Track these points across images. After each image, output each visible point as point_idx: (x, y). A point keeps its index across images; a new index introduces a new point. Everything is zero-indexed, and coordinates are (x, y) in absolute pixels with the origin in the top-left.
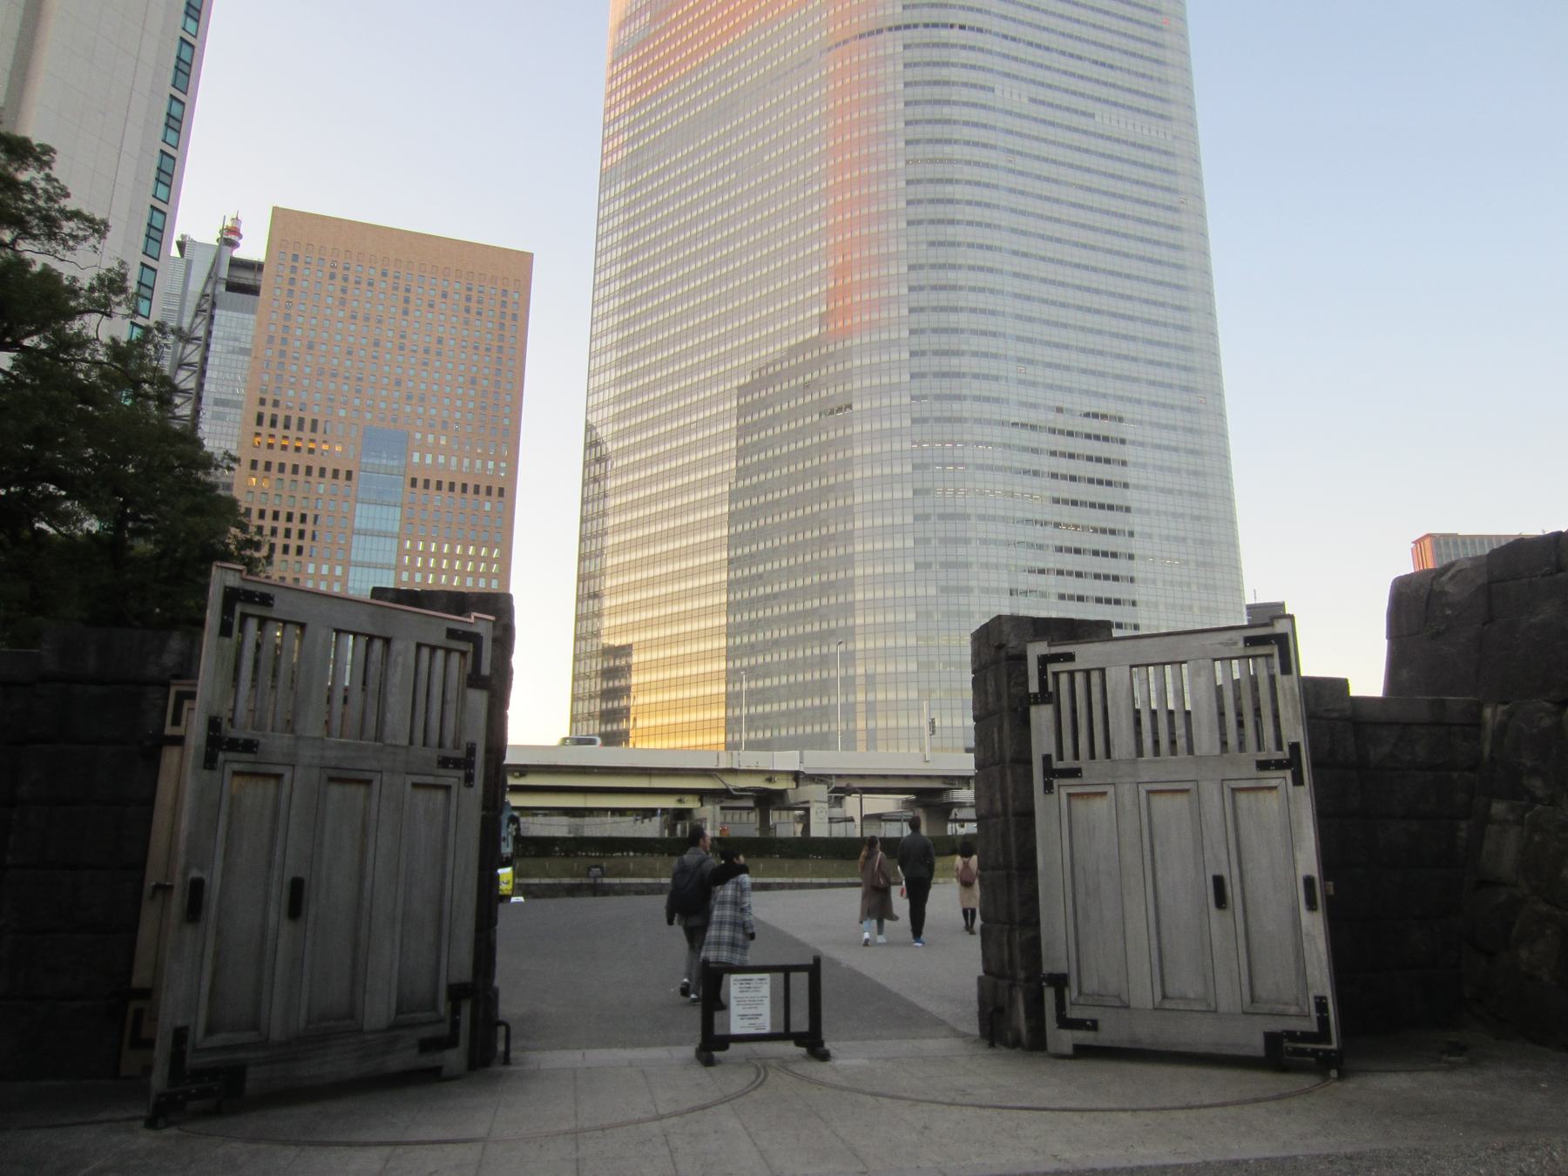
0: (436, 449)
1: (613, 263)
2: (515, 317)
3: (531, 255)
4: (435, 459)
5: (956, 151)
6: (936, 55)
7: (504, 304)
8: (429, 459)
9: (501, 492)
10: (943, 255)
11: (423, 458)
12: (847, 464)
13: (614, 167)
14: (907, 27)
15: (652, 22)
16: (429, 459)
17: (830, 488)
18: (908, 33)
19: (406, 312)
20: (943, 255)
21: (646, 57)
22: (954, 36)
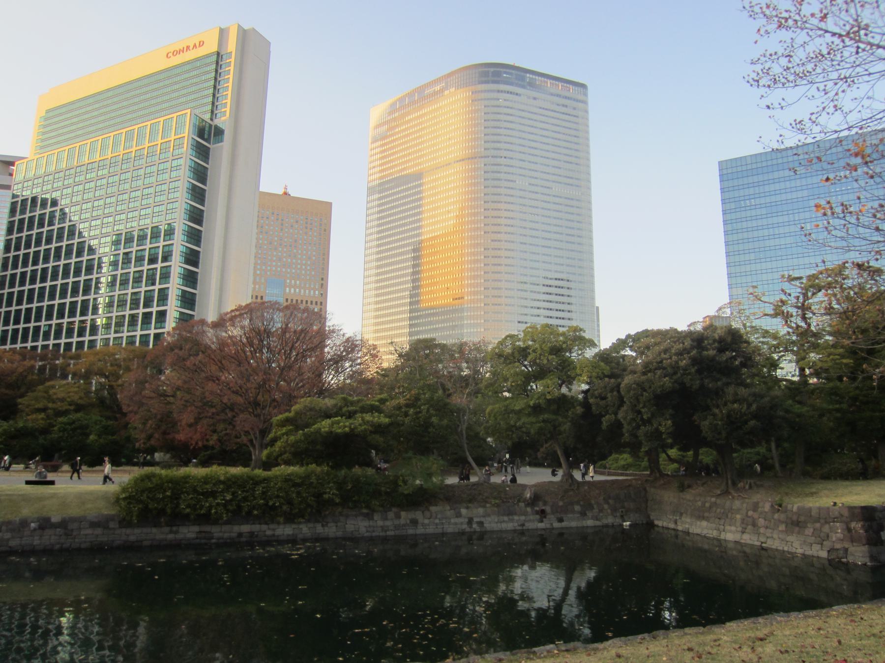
0: (295, 287)
1: (373, 227)
2: (325, 230)
3: (331, 204)
4: (295, 291)
5: (502, 206)
6: (495, 138)
7: (321, 225)
8: (292, 290)
9: (321, 303)
10: (496, 245)
11: (290, 290)
12: (462, 318)
13: (374, 187)
14: (485, 157)
15: (388, 130)
16: (292, 290)
17: (456, 326)
18: (486, 159)
19: (282, 230)
20: (496, 245)
21: (386, 144)
22: (502, 161)
